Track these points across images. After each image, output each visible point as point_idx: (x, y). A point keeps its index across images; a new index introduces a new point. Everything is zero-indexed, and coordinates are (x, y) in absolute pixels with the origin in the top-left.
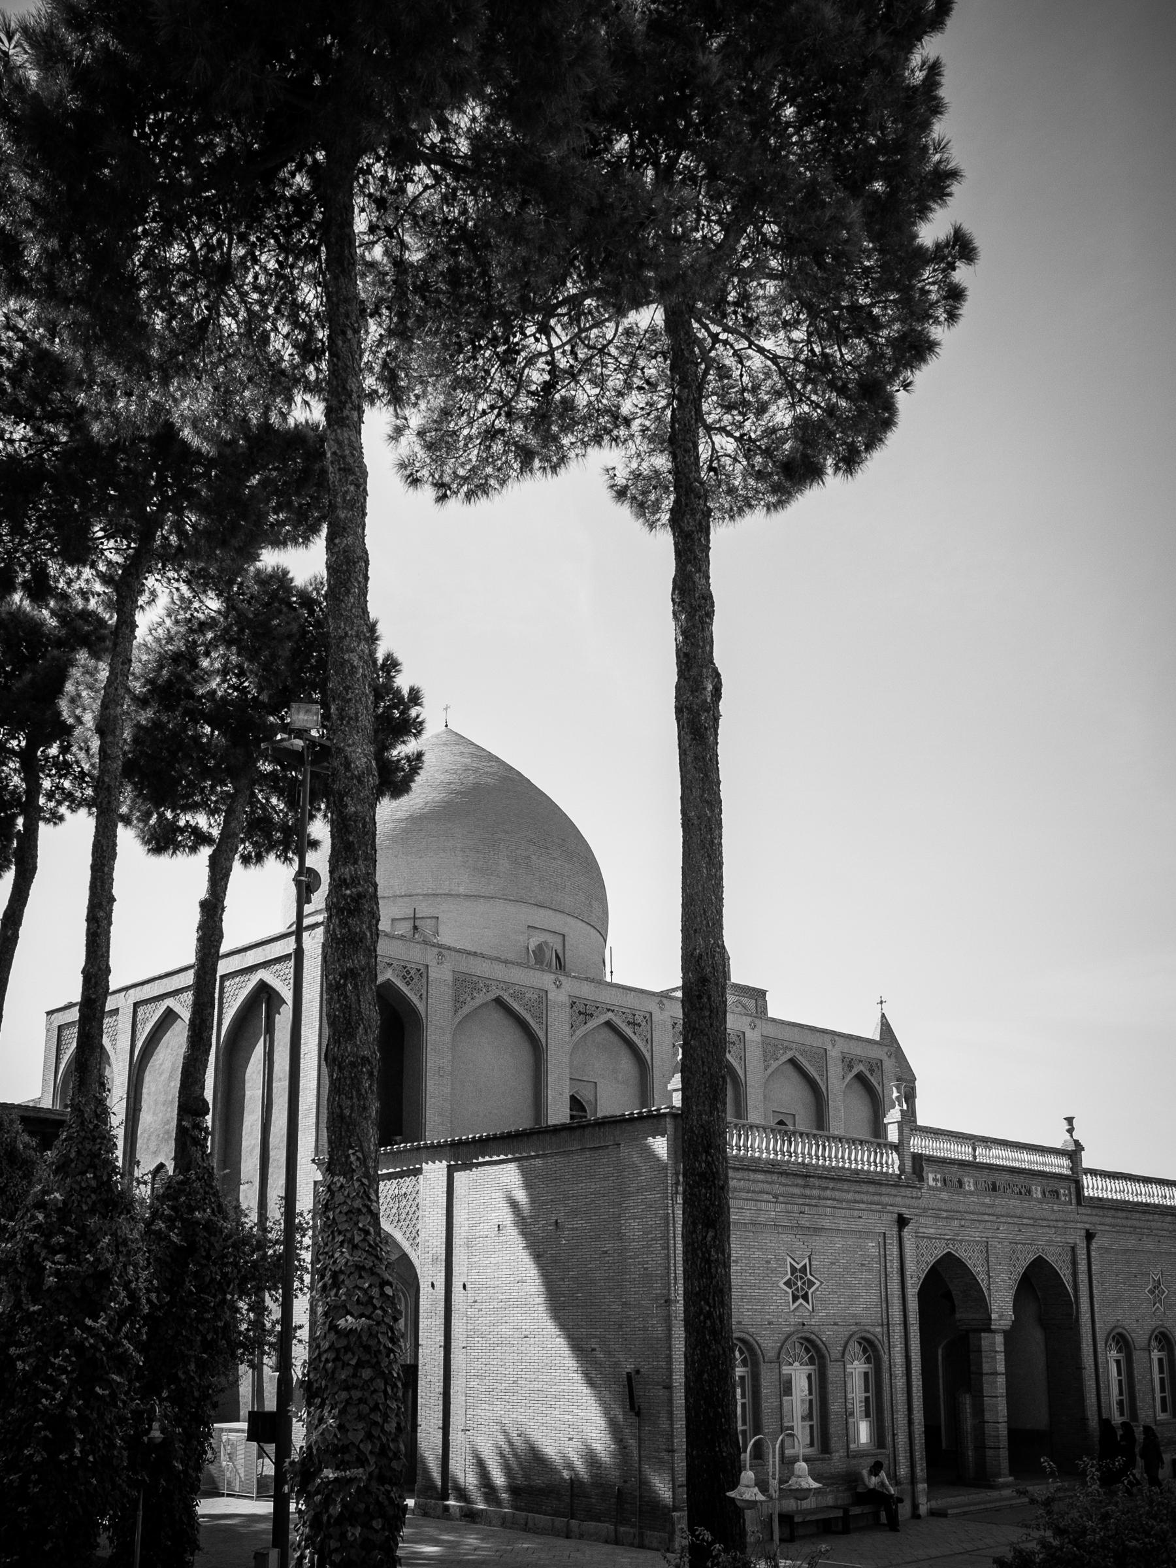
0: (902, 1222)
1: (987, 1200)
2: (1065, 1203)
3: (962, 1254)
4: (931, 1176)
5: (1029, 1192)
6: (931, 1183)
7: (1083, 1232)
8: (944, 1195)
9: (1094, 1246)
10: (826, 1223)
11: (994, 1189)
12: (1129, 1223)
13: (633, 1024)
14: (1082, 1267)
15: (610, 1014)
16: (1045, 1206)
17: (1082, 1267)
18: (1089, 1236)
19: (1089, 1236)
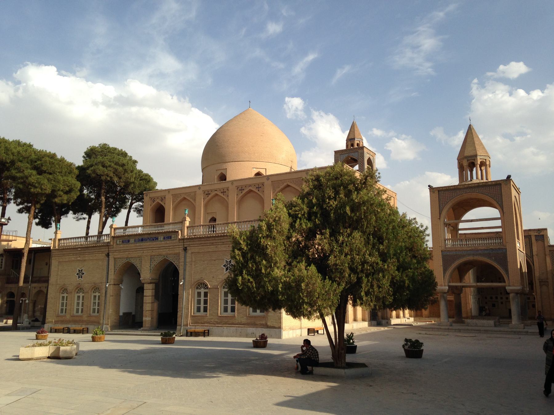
0: (108, 255)
1: (138, 244)
2: (174, 240)
3: (133, 261)
4: (118, 241)
5: (157, 239)
6: (118, 243)
7: (182, 249)
8: (121, 246)
9: (189, 252)
10: (87, 258)
11: (142, 240)
12: (208, 242)
13: (223, 192)
14: (182, 260)
15: (216, 192)
16: (163, 242)
17: (182, 260)
18: (185, 249)
19: (185, 249)
